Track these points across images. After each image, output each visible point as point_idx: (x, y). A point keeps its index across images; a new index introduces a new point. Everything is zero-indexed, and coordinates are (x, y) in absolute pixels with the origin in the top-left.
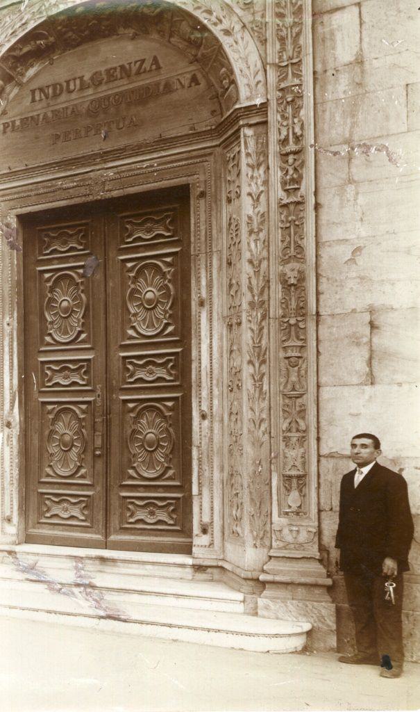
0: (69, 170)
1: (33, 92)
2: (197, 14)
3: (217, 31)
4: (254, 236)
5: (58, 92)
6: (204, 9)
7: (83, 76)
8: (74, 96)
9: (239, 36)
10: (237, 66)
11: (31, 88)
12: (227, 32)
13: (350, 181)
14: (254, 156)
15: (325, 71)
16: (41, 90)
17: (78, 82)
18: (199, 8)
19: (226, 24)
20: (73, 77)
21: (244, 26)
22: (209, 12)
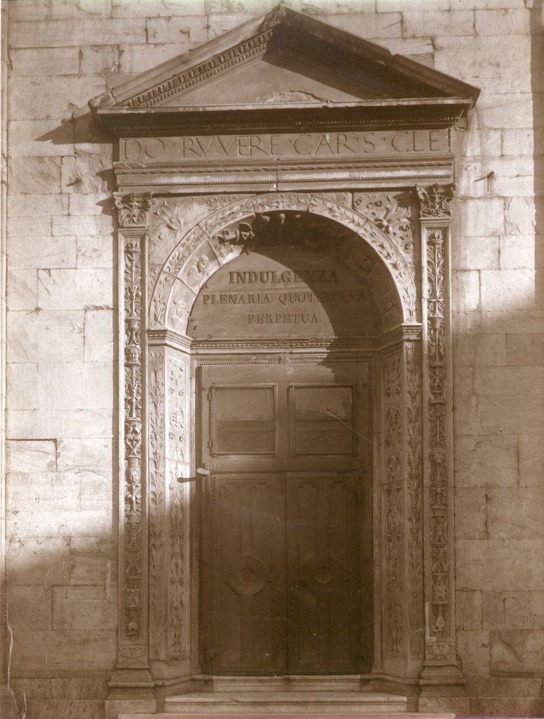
0: (262, 348)
1: (231, 274)
2: (374, 246)
3: (388, 262)
4: (412, 424)
5: (254, 278)
6: (378, 243)
7: (276, 272)
8: (268, 285)
9: (402, 271)
10: (401, 293)
11: (231, 270)
12: (395, 266)
13: (475, 394)
14: (412, 364)
15: (459, 312)
16: (238, 274)
17: (270, 275)
18: (374, 242)
19: (394, 259)
20: (266, 270)
21: (406, 266)
22: (382, 246)
